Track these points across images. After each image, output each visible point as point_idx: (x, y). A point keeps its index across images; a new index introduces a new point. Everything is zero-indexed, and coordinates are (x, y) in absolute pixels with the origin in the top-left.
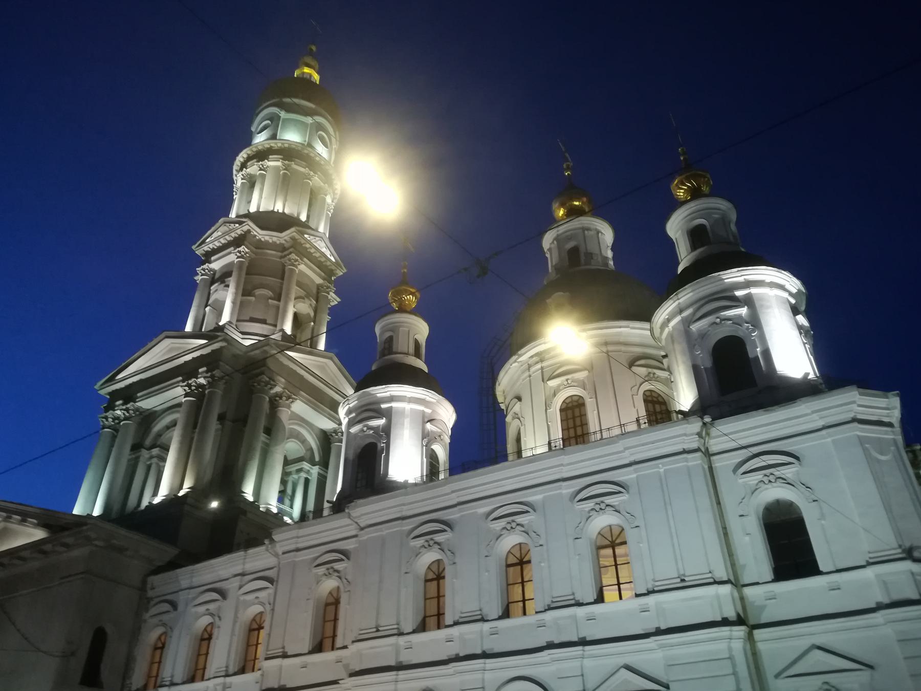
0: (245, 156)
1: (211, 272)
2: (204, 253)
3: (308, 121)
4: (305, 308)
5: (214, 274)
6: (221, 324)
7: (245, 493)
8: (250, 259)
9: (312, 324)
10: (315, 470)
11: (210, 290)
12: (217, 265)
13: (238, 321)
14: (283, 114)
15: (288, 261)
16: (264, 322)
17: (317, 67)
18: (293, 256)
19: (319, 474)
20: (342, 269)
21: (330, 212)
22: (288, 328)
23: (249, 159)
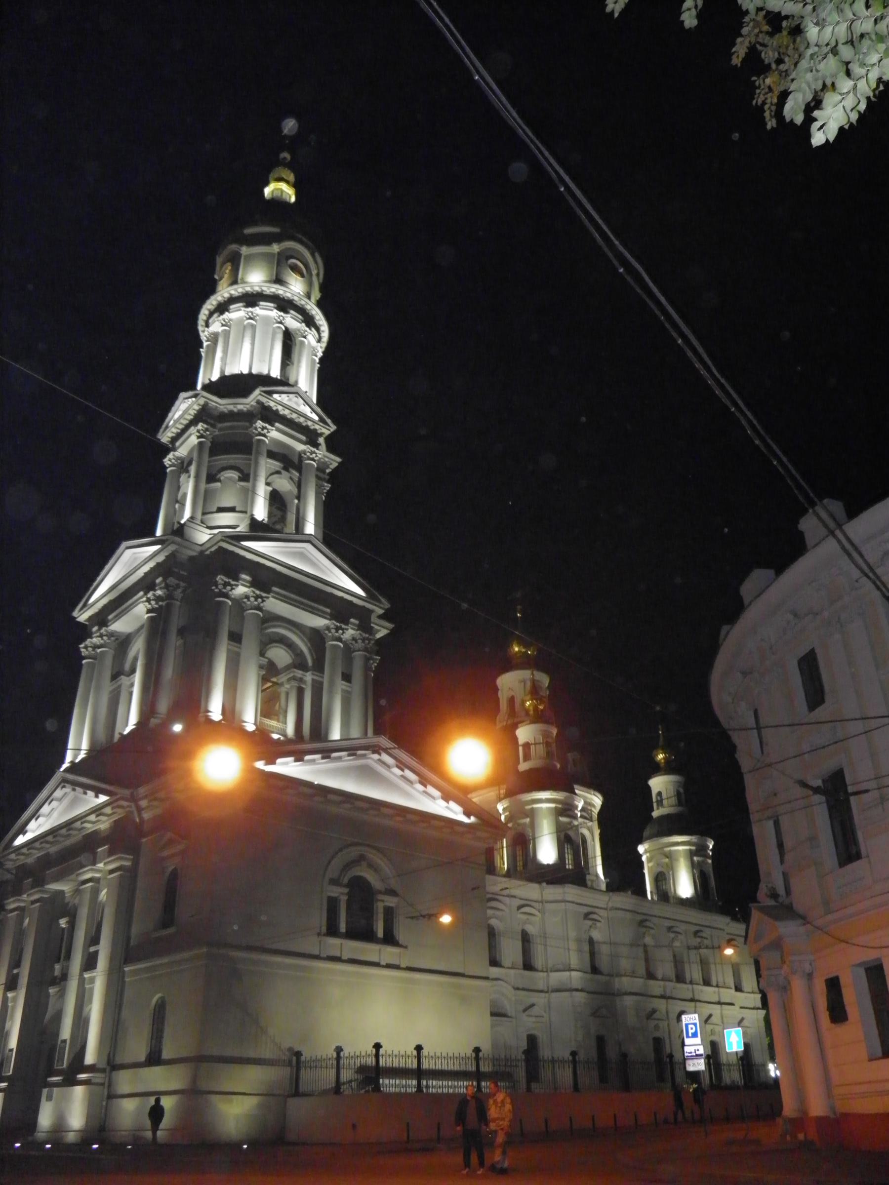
0: (207, 312)
1: (179, 461)
2: (170, 440)
3: (274, 250)
4: (284, 484)
5: (182, 463)
6: (183, 522)
7: (211, 712)
8: (212, 436)
9: (296, 501)
10: (309, 677)
11: (179, 481)
12: (182, 451)
13: (204, 514)
14: (245, 250)
15: (254, 431)
16: (232, 510)
17: (292, 178)
18: (259, 424)
19: (313, 680)
20: (329, 426)
21: (316, 356)
22: (261, 512)
23: (211, 314)
